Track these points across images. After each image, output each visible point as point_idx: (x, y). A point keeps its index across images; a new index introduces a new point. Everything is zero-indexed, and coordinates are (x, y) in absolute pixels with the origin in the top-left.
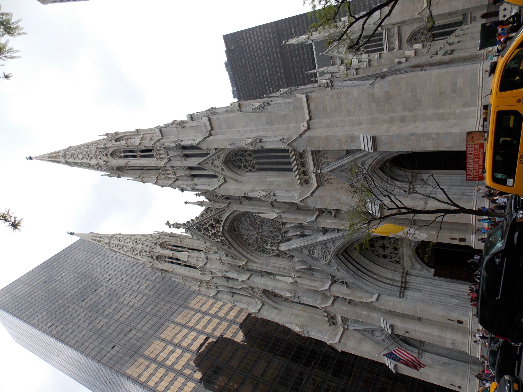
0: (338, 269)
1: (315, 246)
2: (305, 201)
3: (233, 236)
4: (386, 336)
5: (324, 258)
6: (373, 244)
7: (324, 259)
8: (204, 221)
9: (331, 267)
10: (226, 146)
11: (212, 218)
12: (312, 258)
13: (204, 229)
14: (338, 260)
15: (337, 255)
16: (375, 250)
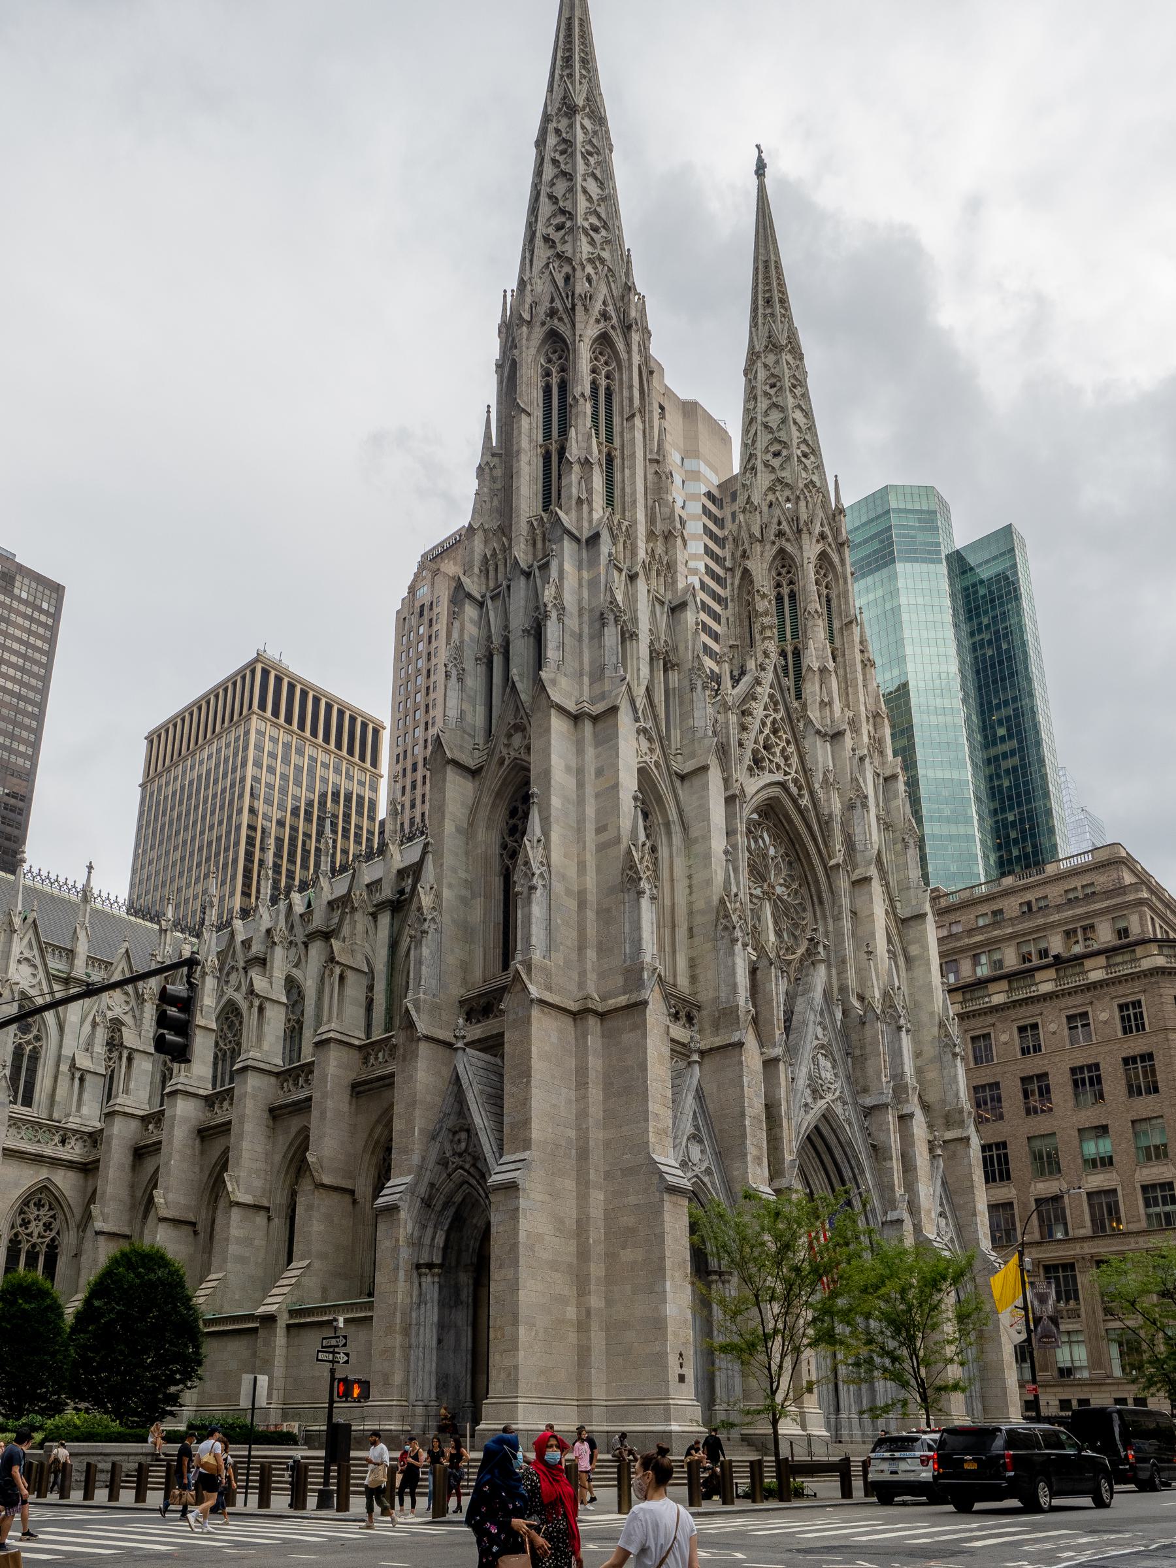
4: (697, 1176)
13: (774, 722)
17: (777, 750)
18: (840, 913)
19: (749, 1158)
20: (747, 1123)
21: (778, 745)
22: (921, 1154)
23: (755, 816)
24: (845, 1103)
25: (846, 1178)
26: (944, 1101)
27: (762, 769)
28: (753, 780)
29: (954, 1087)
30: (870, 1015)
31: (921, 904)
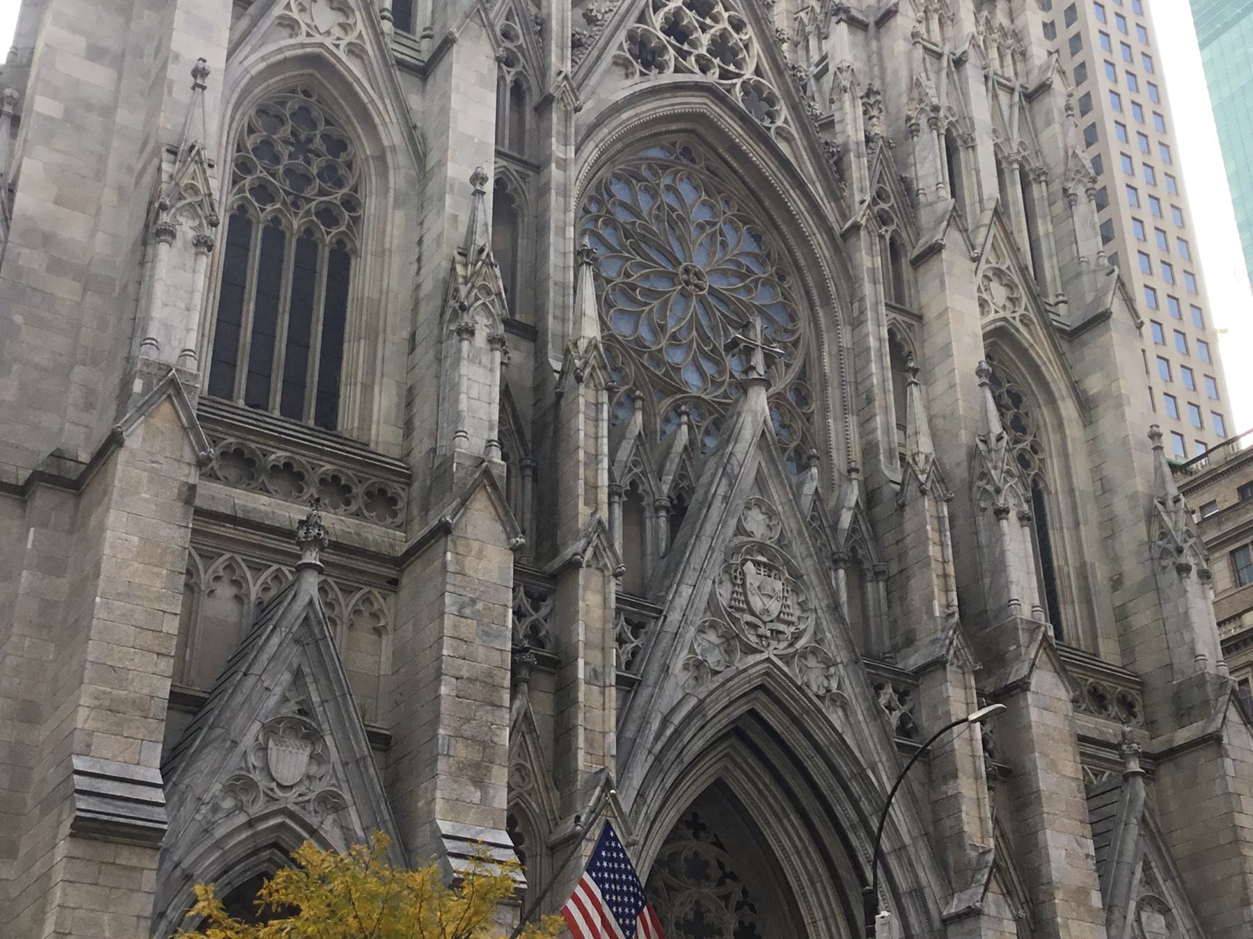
0: (699, 665)
1: (796, 591)
2: (1045, 658)
3: (674, 127)
4: (284, 812)
5: (749, 618)
6: (707, 878)
7: (738, 610)
8: (749, 32)
9: (701, 630)
10: (1129, 403)
11: (770, 84)
12: (737, 549)
14: (747, 688)
15: (762, 687)
16: (673, 873)
17: (705, 39)
18: (862, 312)
19: (442, 765)
20: (443, 690)
21: (704, 29)
22: (1053, 766)
23: (656, 153)
24: (828, 663)
25: (846, 825)
26: (1171, 665)
27: (661, 68)
28: (629, 82)
29: (1187, 638)
30: (912, 489)
31: (1098, 299)
